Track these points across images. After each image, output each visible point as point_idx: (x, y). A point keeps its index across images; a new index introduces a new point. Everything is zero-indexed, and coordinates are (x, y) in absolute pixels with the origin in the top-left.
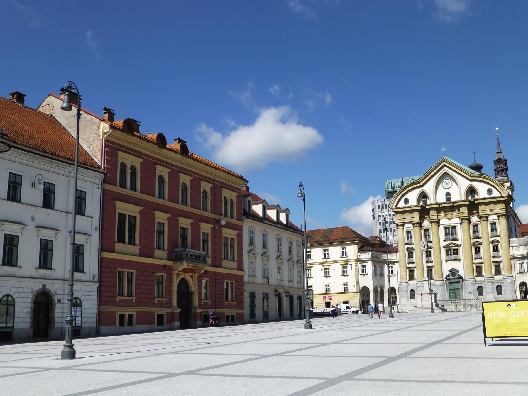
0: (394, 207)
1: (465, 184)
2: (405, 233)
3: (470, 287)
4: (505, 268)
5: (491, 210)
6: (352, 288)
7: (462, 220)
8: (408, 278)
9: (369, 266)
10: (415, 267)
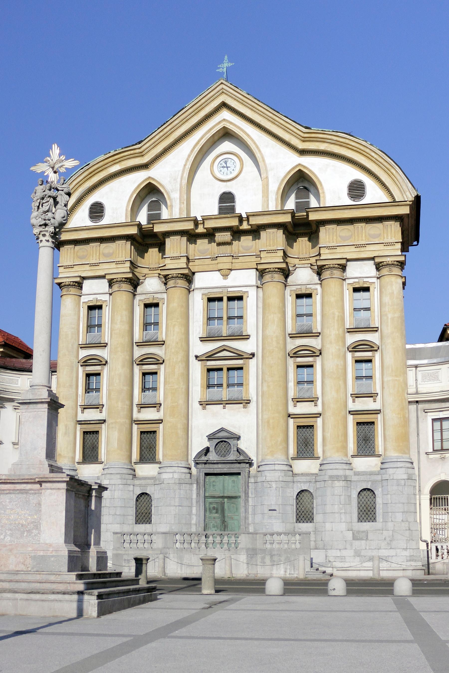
2: (84, 311)
4: (391, 432)
7: (262, 273)
8: (78, 456)
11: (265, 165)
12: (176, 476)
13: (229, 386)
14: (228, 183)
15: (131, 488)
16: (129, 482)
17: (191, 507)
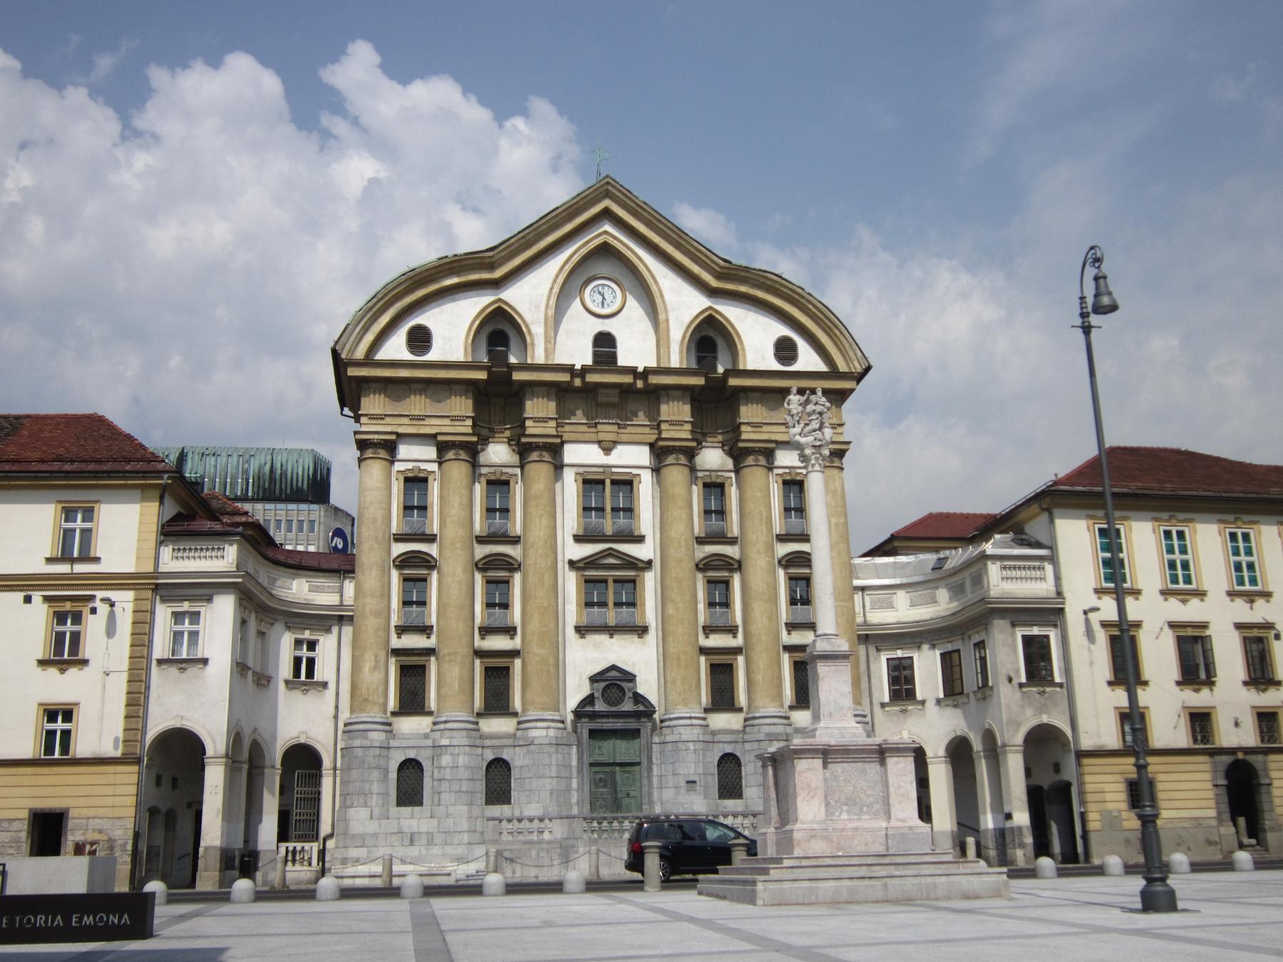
1: (684, 304)
2: (397, 487)
3: (691, 757)
6: (99, 733)
8: (392, 703)
10: (430, 652)
11: (664, 302)
12: (552, 733)
13: (617, 604)
14: (606, 321)
15: (479, 751)
16: (478, 742)
17: (570, 778)
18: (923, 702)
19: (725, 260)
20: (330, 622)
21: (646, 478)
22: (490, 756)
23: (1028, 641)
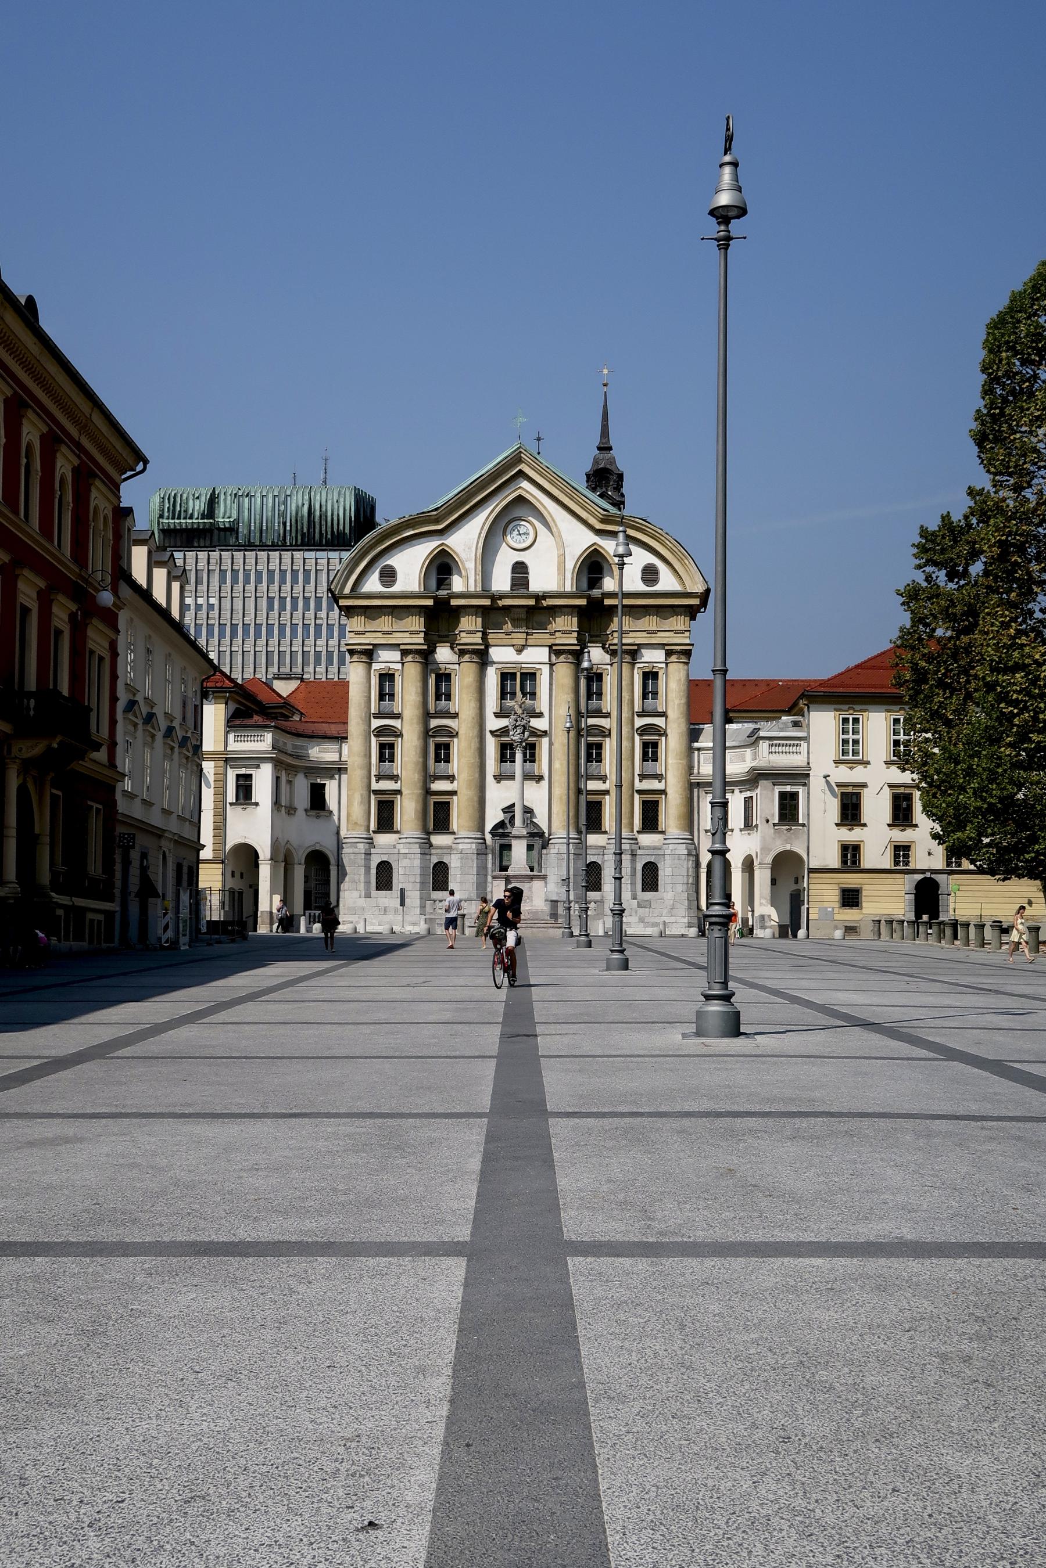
0: (347, 590)
2: (375, 681)
5: (649, 632)
7: (555, 651)
8: (373, 825)
9: (263, 780)
15: (428, 857)
16: (427, 851)
18: (732, 830)
19: (605, 510)
20: (333, 772)
21: (546, 669)
22: (435, 860)
23: (783, 795)
